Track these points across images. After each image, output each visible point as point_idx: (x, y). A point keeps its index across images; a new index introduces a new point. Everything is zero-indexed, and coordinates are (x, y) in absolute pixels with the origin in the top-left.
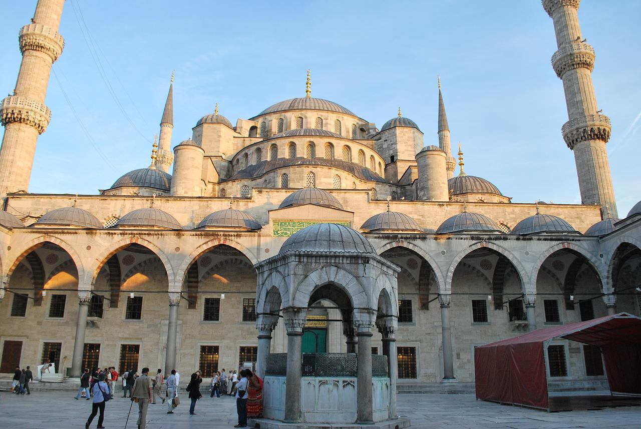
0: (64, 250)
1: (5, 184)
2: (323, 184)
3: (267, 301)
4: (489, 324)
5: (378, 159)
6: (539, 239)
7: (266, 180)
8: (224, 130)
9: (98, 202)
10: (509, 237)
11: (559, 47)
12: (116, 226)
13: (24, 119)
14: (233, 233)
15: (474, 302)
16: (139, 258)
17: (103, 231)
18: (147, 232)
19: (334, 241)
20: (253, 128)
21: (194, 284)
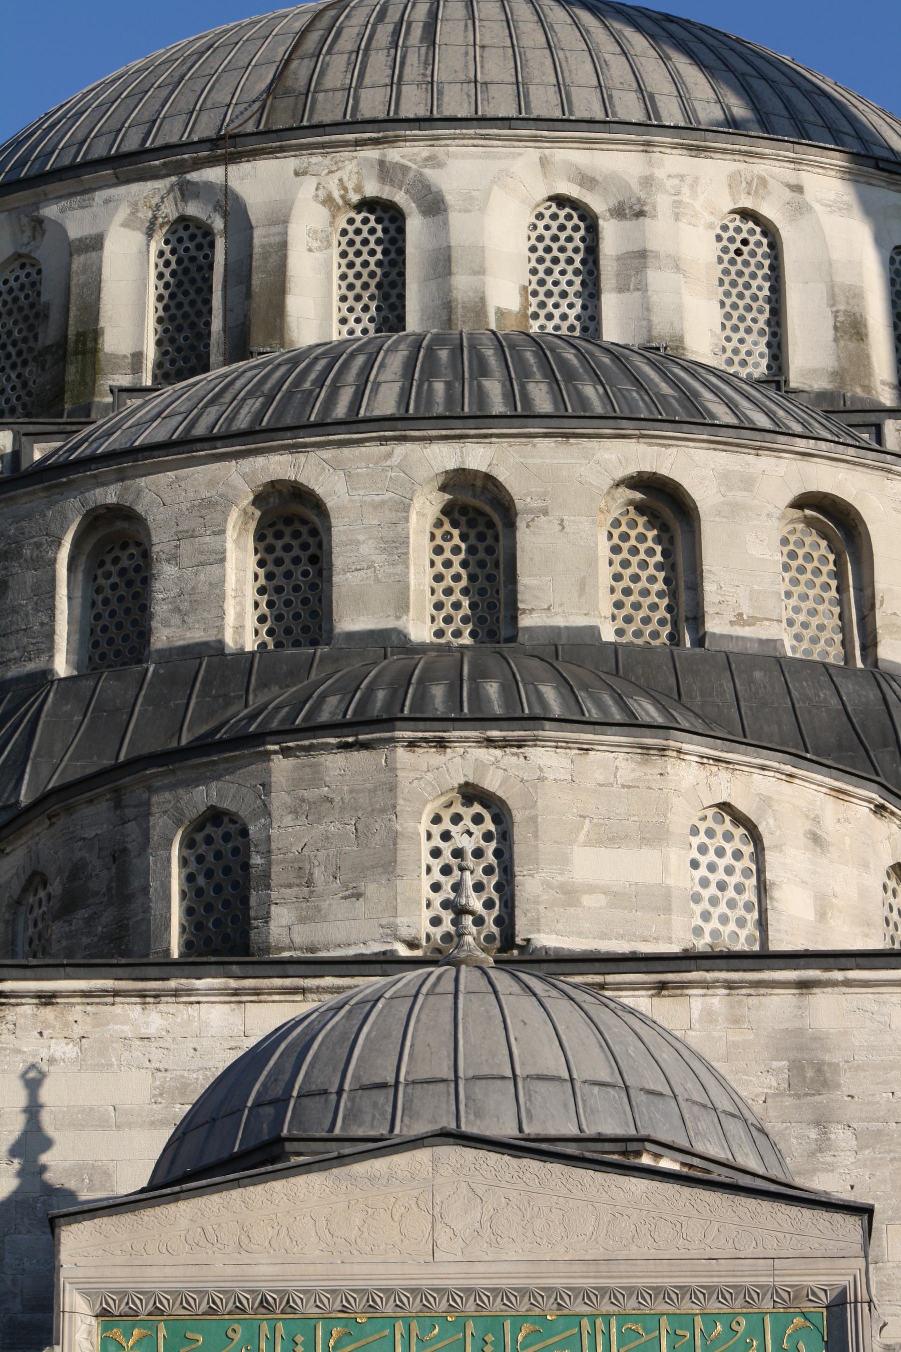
2: (588, 900)
7: (36, 879)
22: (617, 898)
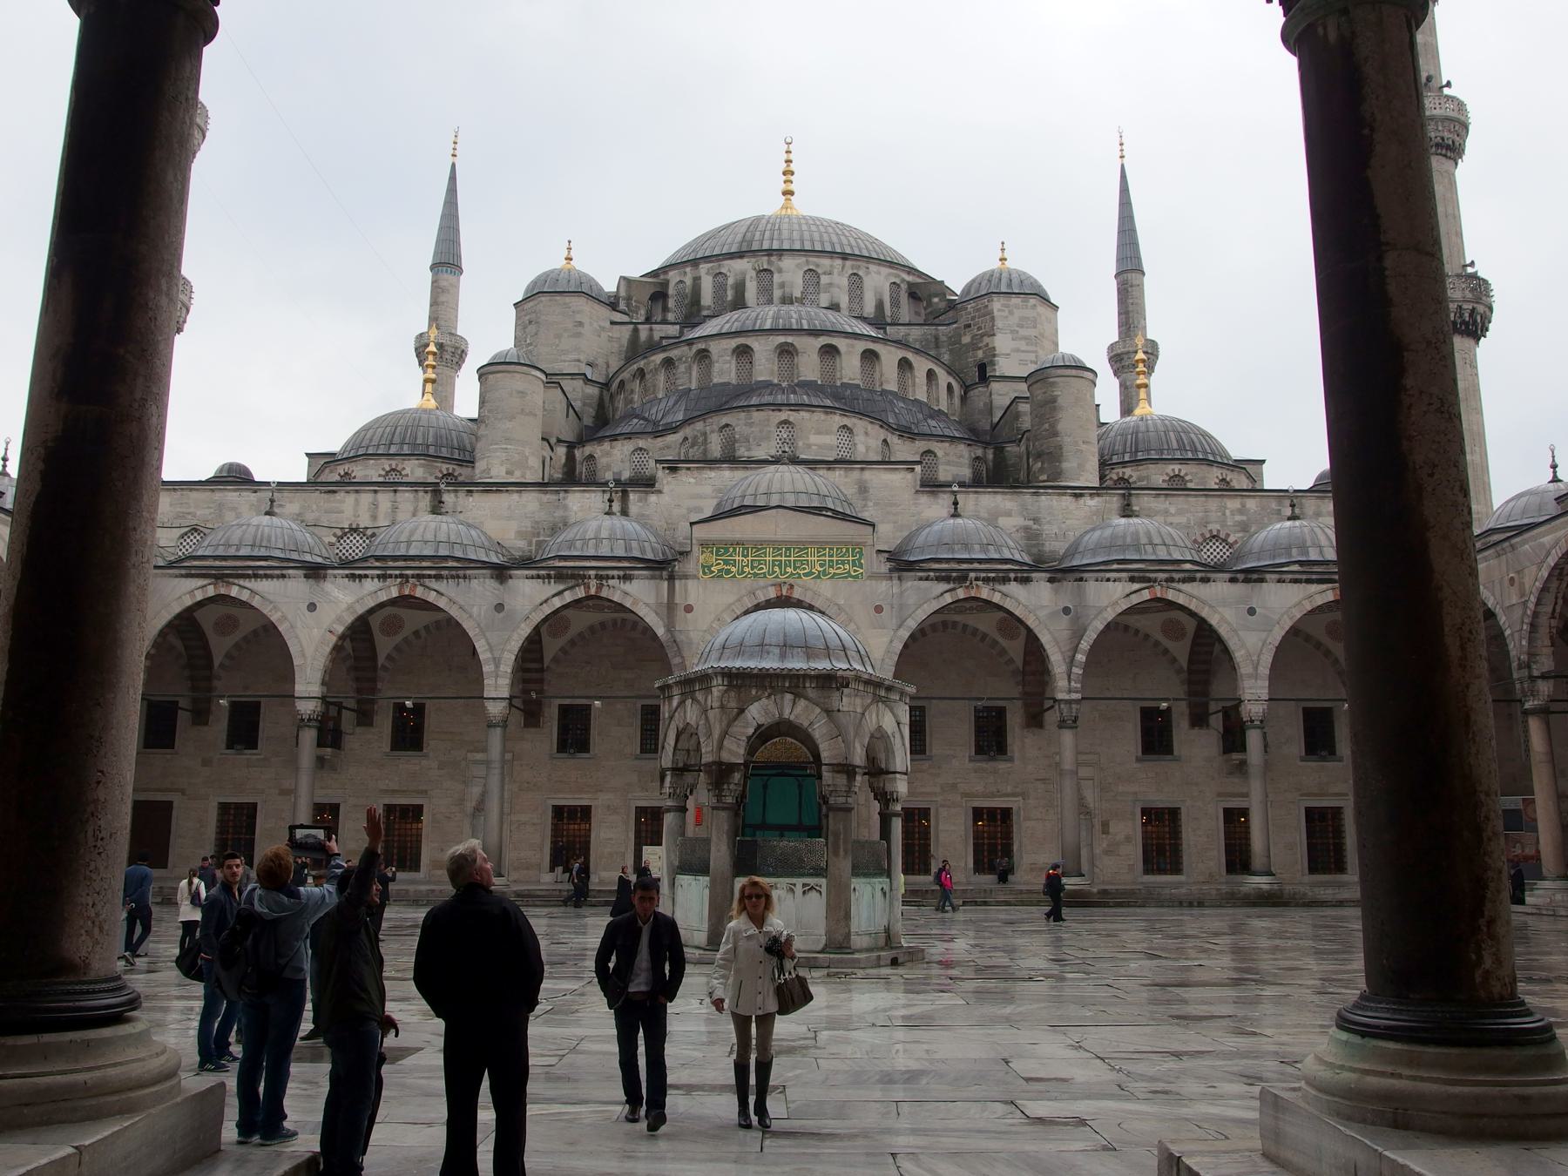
4: (1177, 760)
5: (943, 378)
7: (686, 439)
9: (316, 499)
12: (365, 559)
21: (535, 676)
22: (820, 447)
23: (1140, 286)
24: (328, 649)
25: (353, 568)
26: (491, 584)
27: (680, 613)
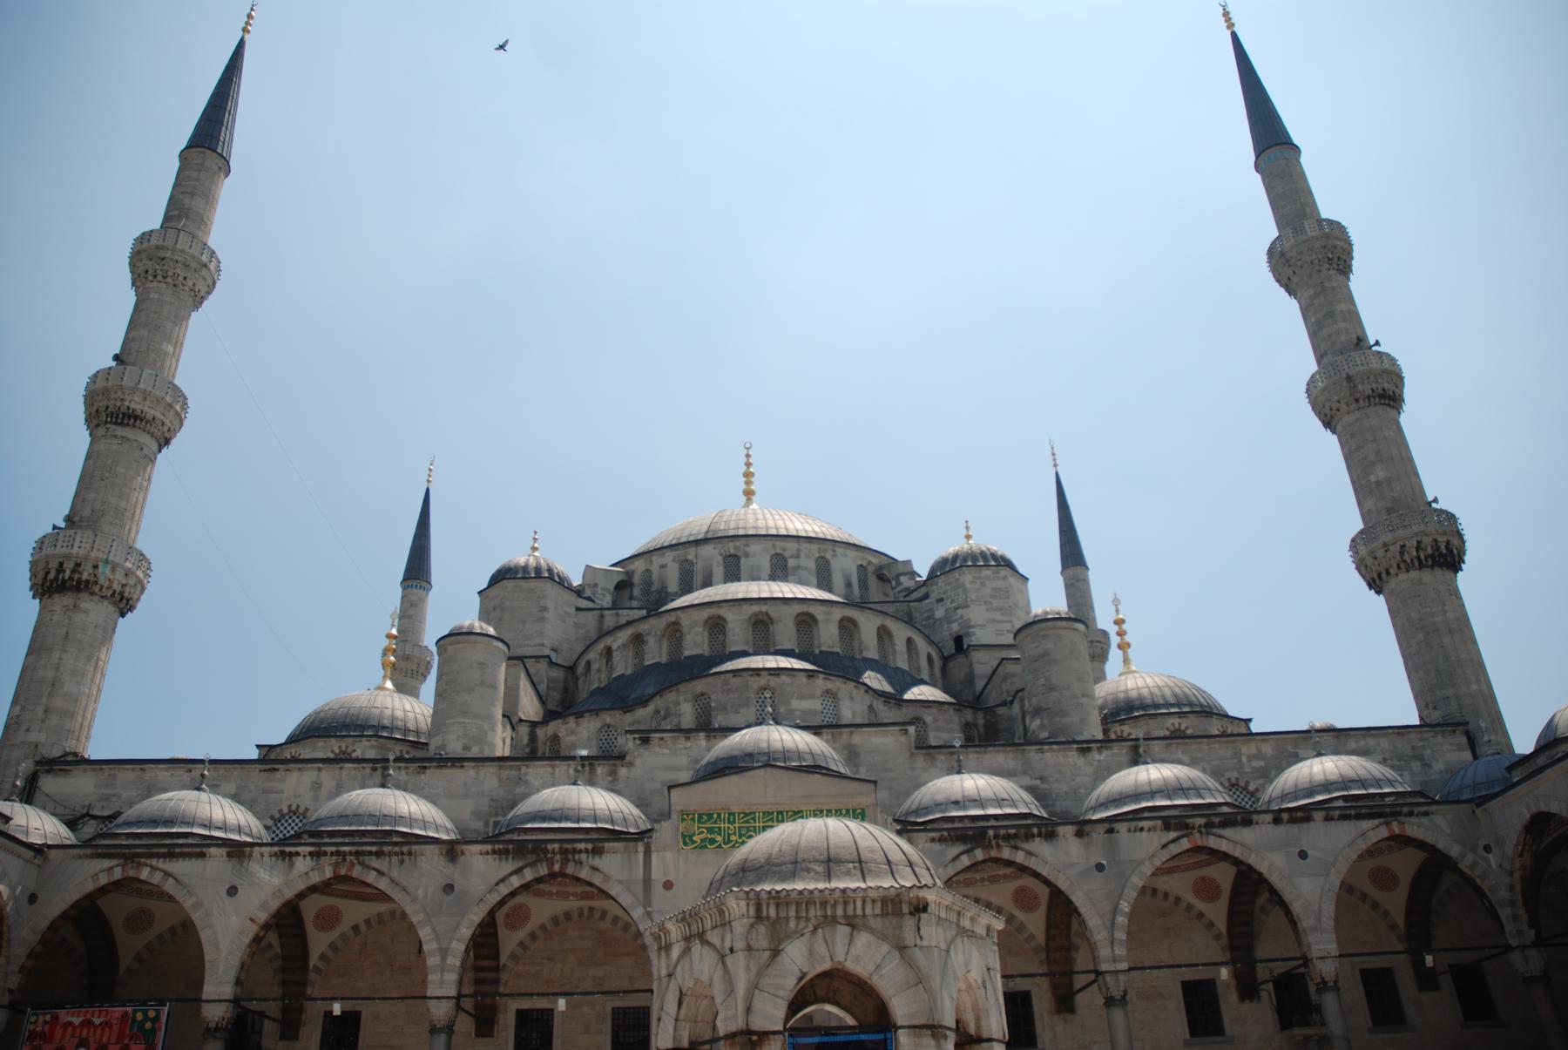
0: (171, 898)
1: (34, 737)
3: (682, 1016)
6: (1328, 819)
7: (657, 712)
8: (551, 590)
9: (256, 777)
10: (1255, 817)
11: (1319, 363)
13: (87, 582)
14: (582, 846)
15: (1190, 989)
16: (355, 912)
17: (268, 849)
18: (374, 849)
19: (839, 861)
20: (623, 586)
22: (805, 712)
23: (1085, 581)
24: (247, 940)
25: (284, 848)
26: (442, 861)
27: (658, 889)
